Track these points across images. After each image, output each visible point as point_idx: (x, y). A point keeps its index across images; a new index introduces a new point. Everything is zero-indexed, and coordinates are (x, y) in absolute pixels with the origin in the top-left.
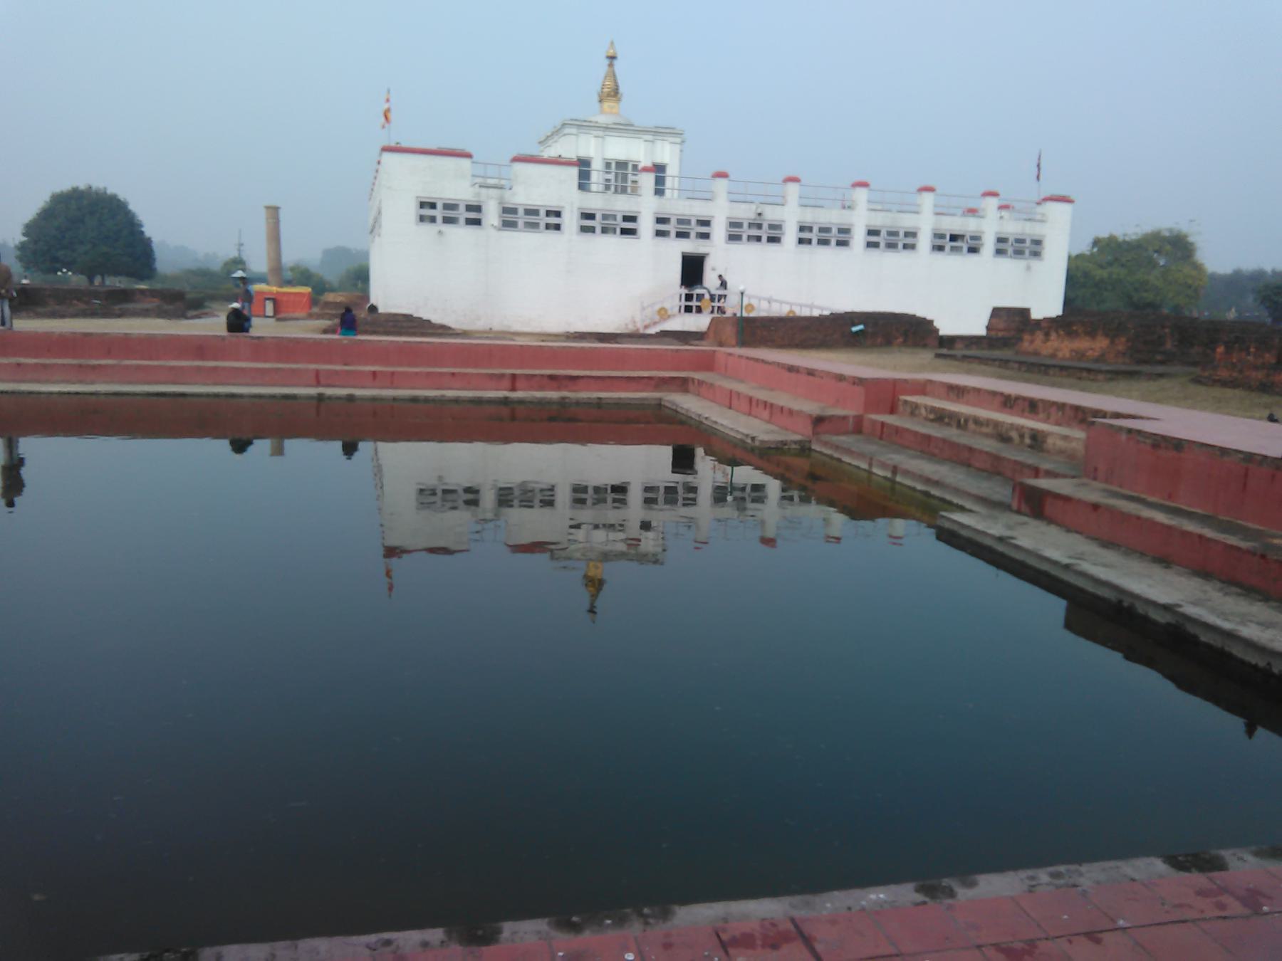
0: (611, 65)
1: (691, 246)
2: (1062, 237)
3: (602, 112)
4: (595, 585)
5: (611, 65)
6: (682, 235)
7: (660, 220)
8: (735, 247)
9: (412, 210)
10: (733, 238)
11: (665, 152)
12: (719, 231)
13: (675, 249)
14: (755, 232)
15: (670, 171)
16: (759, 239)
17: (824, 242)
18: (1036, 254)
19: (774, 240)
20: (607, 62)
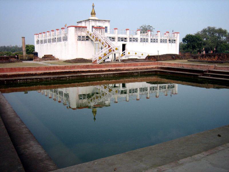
0: (93, 8)
1: (124, 43)
2: (179, 40)
3: (92, 17)
4: (95, 112)
5: (93, 8)
6: (122, 41)
7: (118, 38)
8: (131, 43)
9: (77, 38)
10: (130, 41)
11: (106, 24)
12: (128, 40)
13: (121, 43)
14: (134, 40)
15: (108, 28)
16: (134, 41)
17: (144, 41)
18: (175, 42)
19: (137, 41)
20: (92, 7)
